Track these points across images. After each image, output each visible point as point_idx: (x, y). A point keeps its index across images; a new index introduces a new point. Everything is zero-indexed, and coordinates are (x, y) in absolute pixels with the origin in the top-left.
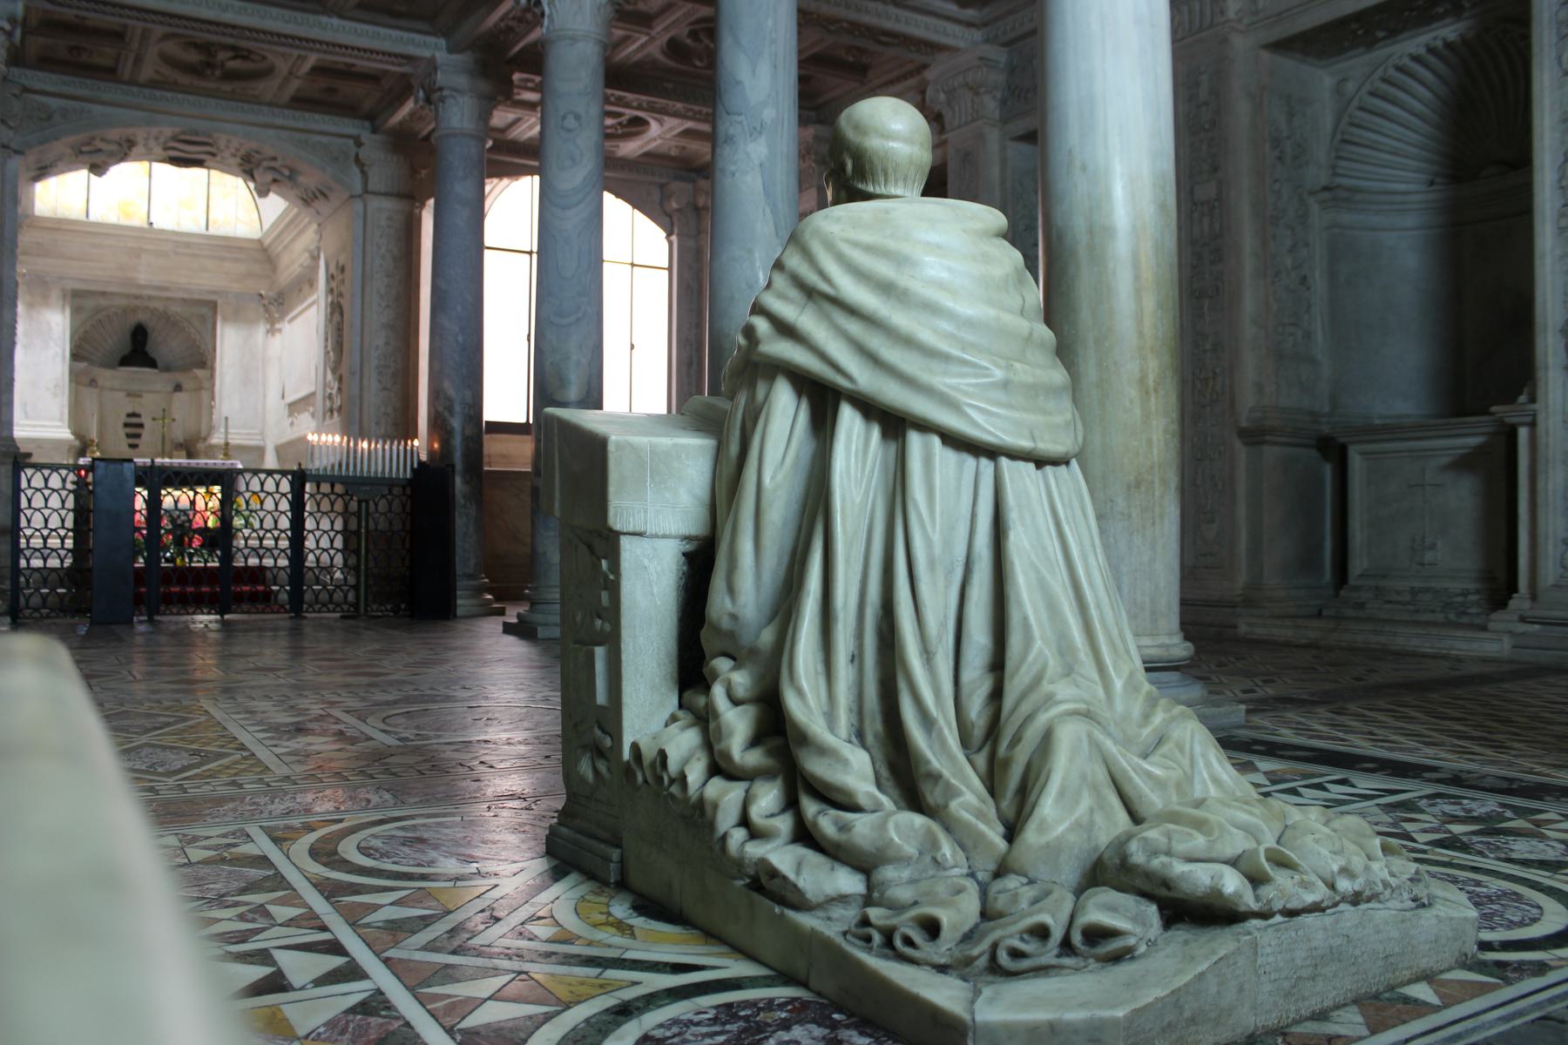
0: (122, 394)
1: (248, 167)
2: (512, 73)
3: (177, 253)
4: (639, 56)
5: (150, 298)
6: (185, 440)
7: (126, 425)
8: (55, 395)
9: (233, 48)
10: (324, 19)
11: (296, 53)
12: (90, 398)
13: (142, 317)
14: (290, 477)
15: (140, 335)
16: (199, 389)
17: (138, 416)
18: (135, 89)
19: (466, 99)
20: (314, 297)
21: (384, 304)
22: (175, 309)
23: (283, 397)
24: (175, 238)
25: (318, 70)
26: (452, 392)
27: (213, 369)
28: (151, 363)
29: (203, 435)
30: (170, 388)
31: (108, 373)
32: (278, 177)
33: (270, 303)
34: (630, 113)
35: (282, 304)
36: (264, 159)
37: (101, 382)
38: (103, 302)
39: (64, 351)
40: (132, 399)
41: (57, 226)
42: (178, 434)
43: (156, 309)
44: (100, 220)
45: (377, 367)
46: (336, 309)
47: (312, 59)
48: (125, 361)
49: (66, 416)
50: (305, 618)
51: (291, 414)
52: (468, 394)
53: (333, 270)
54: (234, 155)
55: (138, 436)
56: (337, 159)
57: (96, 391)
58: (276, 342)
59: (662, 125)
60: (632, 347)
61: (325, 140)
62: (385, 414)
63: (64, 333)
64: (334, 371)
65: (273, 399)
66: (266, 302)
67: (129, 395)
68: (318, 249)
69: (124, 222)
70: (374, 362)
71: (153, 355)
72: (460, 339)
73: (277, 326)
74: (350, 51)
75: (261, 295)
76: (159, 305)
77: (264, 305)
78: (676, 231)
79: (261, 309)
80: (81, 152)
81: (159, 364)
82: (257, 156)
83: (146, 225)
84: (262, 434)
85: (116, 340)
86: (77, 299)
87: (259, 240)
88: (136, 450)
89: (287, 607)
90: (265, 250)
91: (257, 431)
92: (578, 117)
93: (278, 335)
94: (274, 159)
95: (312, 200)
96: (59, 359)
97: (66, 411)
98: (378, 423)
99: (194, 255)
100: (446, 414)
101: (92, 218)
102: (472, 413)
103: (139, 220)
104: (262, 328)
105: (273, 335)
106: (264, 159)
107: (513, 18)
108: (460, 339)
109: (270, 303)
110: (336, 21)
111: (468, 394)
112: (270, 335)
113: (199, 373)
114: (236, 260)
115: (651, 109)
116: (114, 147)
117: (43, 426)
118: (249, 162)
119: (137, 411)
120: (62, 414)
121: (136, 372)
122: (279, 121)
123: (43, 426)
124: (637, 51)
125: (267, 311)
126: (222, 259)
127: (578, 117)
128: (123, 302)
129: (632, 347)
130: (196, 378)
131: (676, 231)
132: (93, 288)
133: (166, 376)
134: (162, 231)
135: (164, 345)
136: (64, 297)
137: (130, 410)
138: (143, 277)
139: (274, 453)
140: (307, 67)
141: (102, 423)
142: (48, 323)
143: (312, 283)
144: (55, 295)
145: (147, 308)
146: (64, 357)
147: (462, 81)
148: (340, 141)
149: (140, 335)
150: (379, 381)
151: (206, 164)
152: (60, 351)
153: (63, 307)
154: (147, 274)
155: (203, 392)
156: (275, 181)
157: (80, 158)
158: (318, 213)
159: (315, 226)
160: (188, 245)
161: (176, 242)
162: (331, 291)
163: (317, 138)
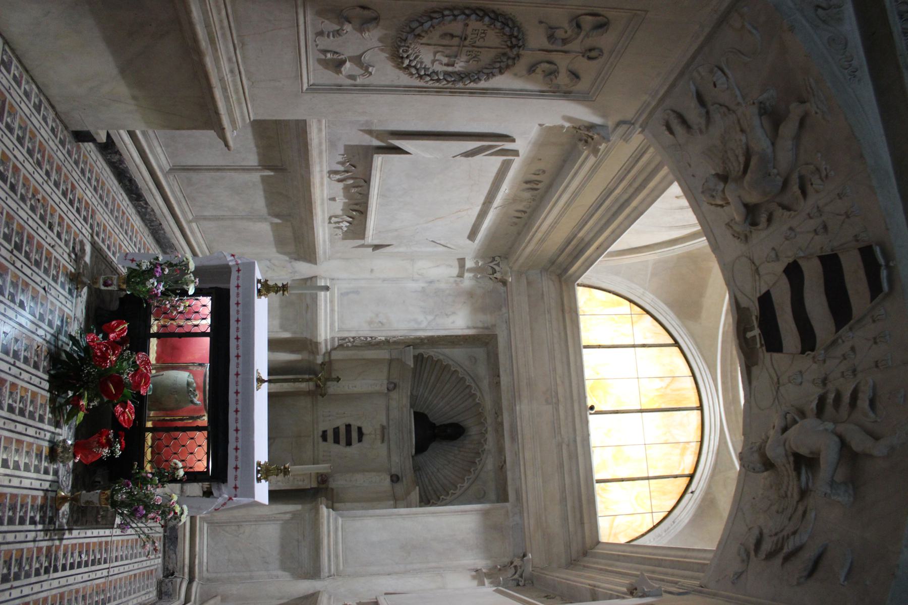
0: (385, 424)
3: (560, 445)
6: (332, 489)
7: (348, 427)
8: (370, 323)
12: (373, 382)
13: (473, 431)
17: (360, 440)
22: (490, 463)
24: (579, 439)
27: (420, 506)
28: (421, 448)
29: (336, 505)
30: (394, 471)
31: (406, 401)
33: (515, 567)
37: (394, 395)
38: (485, 384)
40: (378, 432)
41: (566, 307)
42: (338, 483)
43: (485, 440)
48: (420, 418)
49: (345, 335)
55: (337, 441)
58: (463, 583)
63: (445, 329)
66: (517, 562)
67: (383, 428)
69: (588, 384)
71: (433, 445)
73: (486, 581)
75: (524, 556)
76: (490, 443)
77: (512, 563)
79: (506, 560)
81: (421, 458)
84: (338, 574)
87: (598, 542)
88: (320, 440)
91: (341, 567)
93: (475, 583)
96: (413, 325)
99: (561, 465)
104: (481, 563)
105: (474, 578)
109: (515, 567)
112: (474, 573)
113: (415, 495)
114: (565, 519)
117: (332, 310)
119: (364, 438)
121: (410, 432)
123: (332, 310)
125: (504, 567)
126: (563, 500)
128: (488, 403)
130: (408, 493)
133: (409, 464)
136: (487, 328)
137: (364, 431)
138: (524, 408)
139: (311, 591)
141: (350, 398)
142: (454, 313)
144: (487, 319)
145: (486, 431)
152: (424, 325)
155: (392, 502)
158: (739, 575)
160: (573, 456)
161: (575, 441)
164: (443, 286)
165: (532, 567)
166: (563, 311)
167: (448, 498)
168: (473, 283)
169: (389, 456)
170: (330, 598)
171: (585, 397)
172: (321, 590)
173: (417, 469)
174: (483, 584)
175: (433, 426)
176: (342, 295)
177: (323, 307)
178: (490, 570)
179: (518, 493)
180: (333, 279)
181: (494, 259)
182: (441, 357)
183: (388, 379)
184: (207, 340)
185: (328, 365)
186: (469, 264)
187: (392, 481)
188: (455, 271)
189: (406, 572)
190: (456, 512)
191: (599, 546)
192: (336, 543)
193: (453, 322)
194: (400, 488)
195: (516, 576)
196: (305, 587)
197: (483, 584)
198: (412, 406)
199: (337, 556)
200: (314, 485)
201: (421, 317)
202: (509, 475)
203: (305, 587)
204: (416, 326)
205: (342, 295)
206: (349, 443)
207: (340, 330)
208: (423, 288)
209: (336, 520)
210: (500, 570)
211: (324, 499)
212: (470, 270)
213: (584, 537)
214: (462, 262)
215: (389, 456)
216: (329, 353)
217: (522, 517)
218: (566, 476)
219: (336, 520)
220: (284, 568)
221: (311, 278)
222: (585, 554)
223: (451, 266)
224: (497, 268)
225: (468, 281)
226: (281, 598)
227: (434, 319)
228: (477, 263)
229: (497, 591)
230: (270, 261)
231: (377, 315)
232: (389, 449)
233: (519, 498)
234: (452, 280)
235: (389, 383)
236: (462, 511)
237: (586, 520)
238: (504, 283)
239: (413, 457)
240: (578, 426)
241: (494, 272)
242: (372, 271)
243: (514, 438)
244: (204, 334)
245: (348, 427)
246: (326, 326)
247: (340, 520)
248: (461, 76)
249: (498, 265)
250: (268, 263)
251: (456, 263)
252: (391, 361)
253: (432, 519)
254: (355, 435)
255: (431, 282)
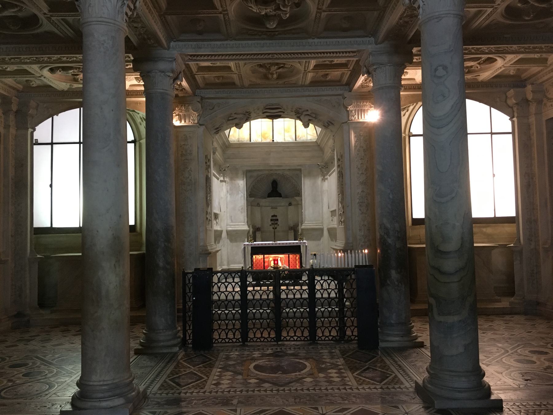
0: (270, 207)
1: (298, 114)
2: (412, 49)
4: (487, 22)
5: (276, 170)
6: (294, 225)
8: (242, 212)
9: (277, 64)
10: (310, 41)
11: (304, 61)
13: (275, 177)
14: (307, 272)
15: (275, 184)
16: (298, 204)
17: (276, 216)
18: (244, 90)
19: (387, 67)
20: (334, 168)
21: (360, 172)
23: (329, 208)
24: (283, 145)
25: (316, 67)
26: (388, 226)
27: (302, 196)
28: (280, 195)
30: (287, 204)
31: (264, 200)
32: (310, 118)
34: (484, 57)
35: (327, 167)
36: (304, 111)
37: (261, 204)
39: (244, 194)
41: (239, 146)
42: (291, 224)
43: (279, 174)
44: (255, 142)
45: (359, 203)
46: (341, 176)
47: (313, 63)
48: (270, 196)
49: (246, 221)
50: (317, 343)
51: (332, 216)
52: (397, 225)
53: (339, 157)
54: (292, 111)
56: (335, 106)
57: (260, 207)
58: (326, 184)
59: (505, 60)
60: (494, 175)
61: (329, 98)
62: (363, 225)
64: (342, 203)
65: (325, 208)
67: (272, 208)
68: (334, 146)
70: (358, 201)
72: (391, 197)
73: (326, 177)
74: (329, 54)
75: (318, 165)
78: (516, 115)
80: (229, 120)
81: (282, 195)
82: (300, 110)
83: (272, 141)
84: (322, 223)
85: (266, 187)
86: (248, 174)
89: (308, 338)
90: (319, 146)
91: (320, 222)
92: (445, 68)
94: (308, 110)
95: (328, 126)
96: (243, 198)
97: (246, 218)
98: (360, 230)
100: (386, 237)
101: (252, 141)
102: (400, 235)
103: (269, 140)
104: (320, 179)
105: (324, 181)
106: (304, 111)
107: (407, 16)
108: (391, 197)
110: (316, 40)
111: (397, 225)
112: (323, 181)
113: (297, 198)
115: (498, 52)
116: (241, 116)
118: (298, 113)
119: (276, 215)
120: (245, 220)
122: (307, 93)
124: (486, 19)
127: (445, 68)
129: (494, 175)
131: (516, 115)
132: (253, 169)
134: (278, 143)
135: (284, 188)
136: (244, 173)
137: (273, 215)
138: (272, 162)
139: (327, 231)
140: (312, 67)
142: (238, 184)
143: (332, 163)
146: (244, 197)
147: (384, 58)
148: (336, 97)
149: (275, 184)
150: (360, 210)
151: (282, 116)
152: (243, 195)
153: (243, 177)
154: (273, 161)
155: (299, 206)
156: (310, 120)
157: (228, 122)
158: (331, 131)
159: (332, 137)
160: (288, 147)
161: (283, 146)
162: (339, 166)
163: (325, 98)
164: (229, 188)
165: (322, 162)
166: (239, 147)
167: (298, 187)
168: (228, 177)
169: (282, 206)
170: (329, 225)
171: (269, 142)
172: (327, 228)
173: (286, 197)
174: (327, 178)
175: (273, 191)
176: (232, 222)
177: (237, 228)
178: (322, 176)
179: (298, 165)
180: (227, 225)
181: (221, 170)
182: (250, 188)
183: (256, 206)
184: (265, 256)
185: (254, 227)
186: (222, 179)
187: (291, 205)
188: (224, 183)
189: (322, 202)
190: (304, 186)
191: (317, 142)
192: (313, 223)
193: (242, 184)
194: (293, 203)
195: (325, 168)
196: (326, 233)
197: (327, 178)
198: (265, 198)
199: (317, 223)
200: (293, 231)
201: (240, 195)
202: (292, 168)
203: (326, 233)
204: (243, 197)
205: (232, 222)
206: (277, 220)
207: (244, 222)
208: (229, 194)
209: (306, 223)
210: (322, 173)
211: (298, 228)
212: (224, 179)
213: (314, 146)
214: (221, 181)
215: (282, 206)
216: (249, 227)
217: (306, 165)
218: (294, 150)
219: (306, 223)
220: (320, 240)
221: (227, 232)
222: (319, 146)
223: (223, 185)
224: (224, 169)
225: (227, 179)
226: (329, 240)
227: (240, 191)
228: (221, 176)
229: (330, 176)
230: (221, 246)
231: (239, 210)
232: (279, 206)
233: (300, 165)
234: (227, 185)
235: (257, 206)
236: (304, 184)
237: (308, 145)
238: (228, 166)
239: (283, 198)
240: (279, 145)
241: (225, 170)
242: (225, 212)
243: (281, 166)
244: (264, 256)
245: (271, 220)
246: (243, 227)
247: (306, 222)
248: (210, 190)
249: (222, 169)
250: (222, 247)
251: (222, 183)
252: (252, 206)
253: (306, 193)
254: (274, 218)
255: (227, 192)
